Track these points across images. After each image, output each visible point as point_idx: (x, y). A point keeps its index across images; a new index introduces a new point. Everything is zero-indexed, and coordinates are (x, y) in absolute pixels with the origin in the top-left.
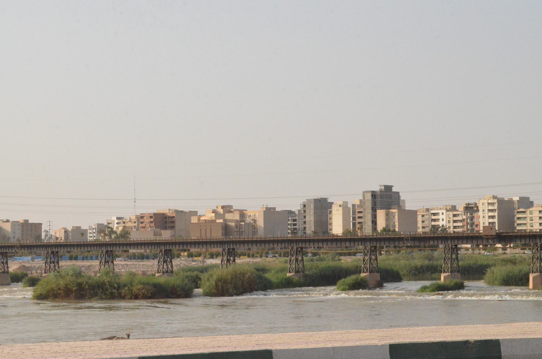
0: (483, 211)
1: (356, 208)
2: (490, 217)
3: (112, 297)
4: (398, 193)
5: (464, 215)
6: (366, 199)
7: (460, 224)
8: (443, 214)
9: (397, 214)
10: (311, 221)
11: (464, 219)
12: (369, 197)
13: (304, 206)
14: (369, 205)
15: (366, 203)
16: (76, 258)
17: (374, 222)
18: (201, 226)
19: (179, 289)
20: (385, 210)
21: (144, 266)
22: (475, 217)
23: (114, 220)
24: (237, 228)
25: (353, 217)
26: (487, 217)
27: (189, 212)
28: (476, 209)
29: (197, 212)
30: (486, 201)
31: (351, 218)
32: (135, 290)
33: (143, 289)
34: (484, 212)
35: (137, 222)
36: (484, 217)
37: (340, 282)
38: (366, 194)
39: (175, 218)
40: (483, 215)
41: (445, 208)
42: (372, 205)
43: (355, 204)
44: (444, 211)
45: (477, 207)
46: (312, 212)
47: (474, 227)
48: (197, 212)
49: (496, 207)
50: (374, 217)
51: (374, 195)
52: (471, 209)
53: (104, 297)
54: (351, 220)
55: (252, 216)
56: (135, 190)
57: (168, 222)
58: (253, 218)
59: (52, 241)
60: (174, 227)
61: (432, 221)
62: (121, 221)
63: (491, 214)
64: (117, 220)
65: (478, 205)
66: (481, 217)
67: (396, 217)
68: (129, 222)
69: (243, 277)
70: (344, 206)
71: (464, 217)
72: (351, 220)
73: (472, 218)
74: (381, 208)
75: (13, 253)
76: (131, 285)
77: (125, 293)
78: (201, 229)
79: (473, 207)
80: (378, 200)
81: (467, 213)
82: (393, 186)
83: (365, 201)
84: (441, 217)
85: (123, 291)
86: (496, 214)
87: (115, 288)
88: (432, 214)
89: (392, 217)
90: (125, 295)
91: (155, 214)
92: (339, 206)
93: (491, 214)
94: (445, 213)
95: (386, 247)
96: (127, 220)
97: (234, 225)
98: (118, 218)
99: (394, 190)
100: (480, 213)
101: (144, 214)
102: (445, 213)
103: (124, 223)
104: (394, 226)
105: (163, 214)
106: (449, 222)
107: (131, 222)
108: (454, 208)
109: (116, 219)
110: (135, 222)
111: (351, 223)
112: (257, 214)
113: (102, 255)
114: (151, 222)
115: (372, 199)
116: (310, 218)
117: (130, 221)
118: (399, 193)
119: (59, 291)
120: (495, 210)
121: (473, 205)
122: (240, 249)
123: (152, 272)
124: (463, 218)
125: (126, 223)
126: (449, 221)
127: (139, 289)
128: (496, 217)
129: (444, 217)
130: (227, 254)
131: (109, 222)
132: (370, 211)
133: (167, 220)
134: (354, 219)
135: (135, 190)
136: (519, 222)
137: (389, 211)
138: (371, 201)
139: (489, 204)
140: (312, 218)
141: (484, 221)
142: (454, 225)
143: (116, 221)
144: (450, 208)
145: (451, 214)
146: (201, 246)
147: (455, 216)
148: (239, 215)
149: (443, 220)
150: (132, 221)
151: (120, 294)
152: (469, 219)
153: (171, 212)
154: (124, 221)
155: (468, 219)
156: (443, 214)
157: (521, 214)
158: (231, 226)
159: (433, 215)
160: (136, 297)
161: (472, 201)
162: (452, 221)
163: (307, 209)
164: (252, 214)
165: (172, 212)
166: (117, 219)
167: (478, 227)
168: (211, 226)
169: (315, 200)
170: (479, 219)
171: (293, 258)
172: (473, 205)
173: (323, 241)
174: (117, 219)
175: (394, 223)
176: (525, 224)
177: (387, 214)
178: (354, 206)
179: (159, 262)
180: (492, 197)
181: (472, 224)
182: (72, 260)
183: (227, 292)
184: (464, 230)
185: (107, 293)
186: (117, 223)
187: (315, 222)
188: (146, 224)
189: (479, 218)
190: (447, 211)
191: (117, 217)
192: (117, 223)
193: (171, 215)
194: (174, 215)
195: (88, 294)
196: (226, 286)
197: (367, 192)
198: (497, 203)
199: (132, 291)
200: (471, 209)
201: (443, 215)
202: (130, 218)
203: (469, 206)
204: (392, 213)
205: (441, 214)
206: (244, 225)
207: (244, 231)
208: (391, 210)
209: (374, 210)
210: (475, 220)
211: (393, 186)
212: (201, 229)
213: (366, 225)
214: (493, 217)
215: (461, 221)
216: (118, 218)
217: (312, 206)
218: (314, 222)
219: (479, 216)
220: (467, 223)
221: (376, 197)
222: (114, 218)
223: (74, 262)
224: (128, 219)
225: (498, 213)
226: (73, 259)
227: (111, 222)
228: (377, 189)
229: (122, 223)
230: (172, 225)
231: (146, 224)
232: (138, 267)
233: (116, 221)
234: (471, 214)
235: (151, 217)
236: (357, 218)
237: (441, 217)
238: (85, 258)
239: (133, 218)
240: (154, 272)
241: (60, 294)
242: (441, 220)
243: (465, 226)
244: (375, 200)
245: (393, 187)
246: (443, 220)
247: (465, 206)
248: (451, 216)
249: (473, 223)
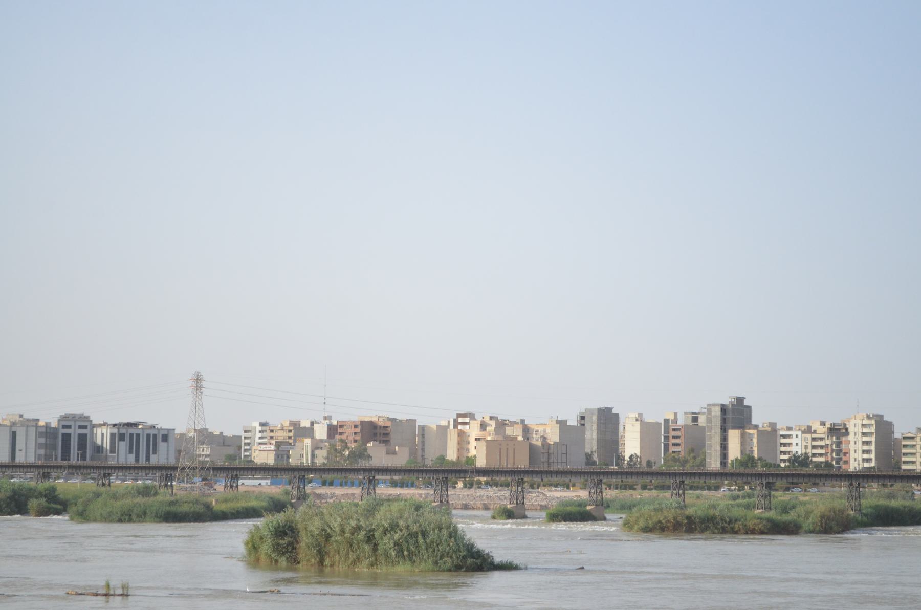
0: (855, 434)
1: (670, 424)
2: (864, 443)
3: (724, 531)
5: (828, 439)
6: (713, 414)
7: (823, 451)
8: (797, 436)
9: (756, 436)
10: (592, 439)
11: (828, 444)
12: (717, 411)
13: (583, 418)
14: (717, 422)
15: (713, 420)
16: (331, 484)
17: (724, 447)
18: (500, 445)
19: (792, 525)
20: (740, 431)
21: (469, 496)
22: (843, 443)
23: (256, 427)
24: (544, 449)
25: (664, 436)
26: (860, 444)
27: (407, 420)
28: (844, 431)
29: (416, 420)
30: (859, 422)
31: (663, 437)
32: (750, 524)
33: (761, 523)
34: (856, 437)
35: (293, 431)
36: (855, 443)
38: (713, 408)
39: (389, 429)
40: (855, 440)
41: (798, 429)
42: (721, 423)
43: (669, 419)
44: (799, 433)
45: (847, 429)
46: (595, 426)
47: (842, 455)
48: (416, 420)
49: (873, 430)
51: (724, 409)
52: (838, 431)
53: (716, 531)
54: (663, 441)
55: (540, 431)
56: (325, 386)
57: (378, 435)
58: (542, 435)
59: (523, 467)
60: (389, 441)
61: (781, 446)
62: (264, 428)
63: (866, 439)
64: (260, 427)
65: (847, 426)
66: (852, 443)
67: (755, 440)
68: (280, 431)
69: (843, 514)
70: (639, 418)
71: (828, 442)
72: (661, 440)
73: (839, 444)
74: (734, 428)
76: (746, 520)
77: (739, 527)
78: (500, 449)
79: (840, 429)
80: (729, 416)
81: (832, 436)
82: (745, 398)
83: (711, 418)
84: (793, 441)
85: (736, 526)
86: (873, 439)
87: (726, 522)
88: (781, 435)
89: (749, 440)
90: (740, 530)
91: (362, 423)
92: (635, 420)
93: (866, 439)
94: (800, 436)
95: (805, 483)
96: (277, 427)
97: (540, 445)
98: (262, 425)
99: (746, 403)
100: (851, 437)
101: (345, 422)
102: (800, 436)
103: (272, 431)
104: (752, 452)
106: (806, 447)
107: (283, 431)
109: (258, 424)
110: (290, 431)
111: (662, 445)
112: (548, 430)
113: (39, 477)
114: (355, 433)
115: (721, 414)
116: (591, 436)
117: (282, 429)
118: (751, 408)
119: (669, 524)
120: (870, 434)
121: (841, 426)
122: (779, 483)
123: (496, 505)
124: (827, 443)
125: (276, 432)
126: (805, 446)
127: (755, 524)
128: (874, 444)
129: (799, 441)
130: (764, 488)
131: (247, 430)
133: (378, 431)
134: (666, 438)
135: (325, 386)
136: (904, 451)
137: (744, 431)
138: (720, 418)
139: (863, 425)
140: (595, 436)
141: (856, 448)
142: (813, 452)
143: (259, 428)
144: (804, 429)
145: (809, 436)
146: (664, 477)
147: (814, 439)
148: (522, 429)
149: (797, 444)
150: (285, 428)
151: (732, 528)
152: (834, 445)
153: (381, 419)
154: (271, 429)
155: (832, 444)
156: (797, 436)
157: (908, 440)
158: (536, 445)
159: (783, 438)
160: (753, 532)
161: (838, 421)
162: (810, 447)
163: (586, 422)
164: (540, 429)
165: (384, 420)
167: (847, 455)
168: (507, 445)
169: (598, 409)
170: (850, 445)
171: (514, 489)
172: (841, 426)
173: (890, 477)
175: (751, 448)
176: (914, 454)
177: (743, 436)
178: (666, 421)
179: (363, 489)
180: (865, 416)
181: (838, 452)
182: (325, 485)
183: (831, 528)
184: (827, 459)
185: (719, 527)
186: (260, 432)
187: (599, 441)
188: (347, 437)
189: (849, 443)
190: (804, 432)
191: (260, 423)
192: (260, 432)
194: (388, 424)
195: (698, 529)
196: (401, 530)
197: (714, 405)
198: (874, 426)
199: (746, 525)
200: (838, 431)
201: (797, 439)
202: (282, 424)
203: (836, 427)
204: (749, 434)
205: (794, 436)
206: (554, 444)
207: (553, 453)
208: (747, 431)
209: (724, 430)
210: (843, 446)
211: (745, 398)
212: (500, 449)
213: (712, 449)
214: (868, 443)
215: (822, 447)
216: (262, 425)
217: (595, 418)
218: (598, 441)
219: (849, 441)
220: (832, 451)
221: (727, 413)
222: (256, 424)
223: (628, 493)
224: (279, 426)
225: (876, 438)
226: (327, 484)
227: (250, 430)
228: (726, 401)
229: (269, 431)
230: (385, 439)
231: (347, 437)
232: (462, 499)
233: (259, 428)
234: (838, 438)
235: (356, 426)
236: (671, 438)
237: (793, 441)
238: (344, 484)
239: (287, 424)
240: (498, 506)
241: (668, 528)
242: (794, 444)
243: (829, 454)
244: (725, 416)
245: (745, 400)
246: (797, 444)
247: (829, 426)
248: (810, 440)
249: (841, 451)
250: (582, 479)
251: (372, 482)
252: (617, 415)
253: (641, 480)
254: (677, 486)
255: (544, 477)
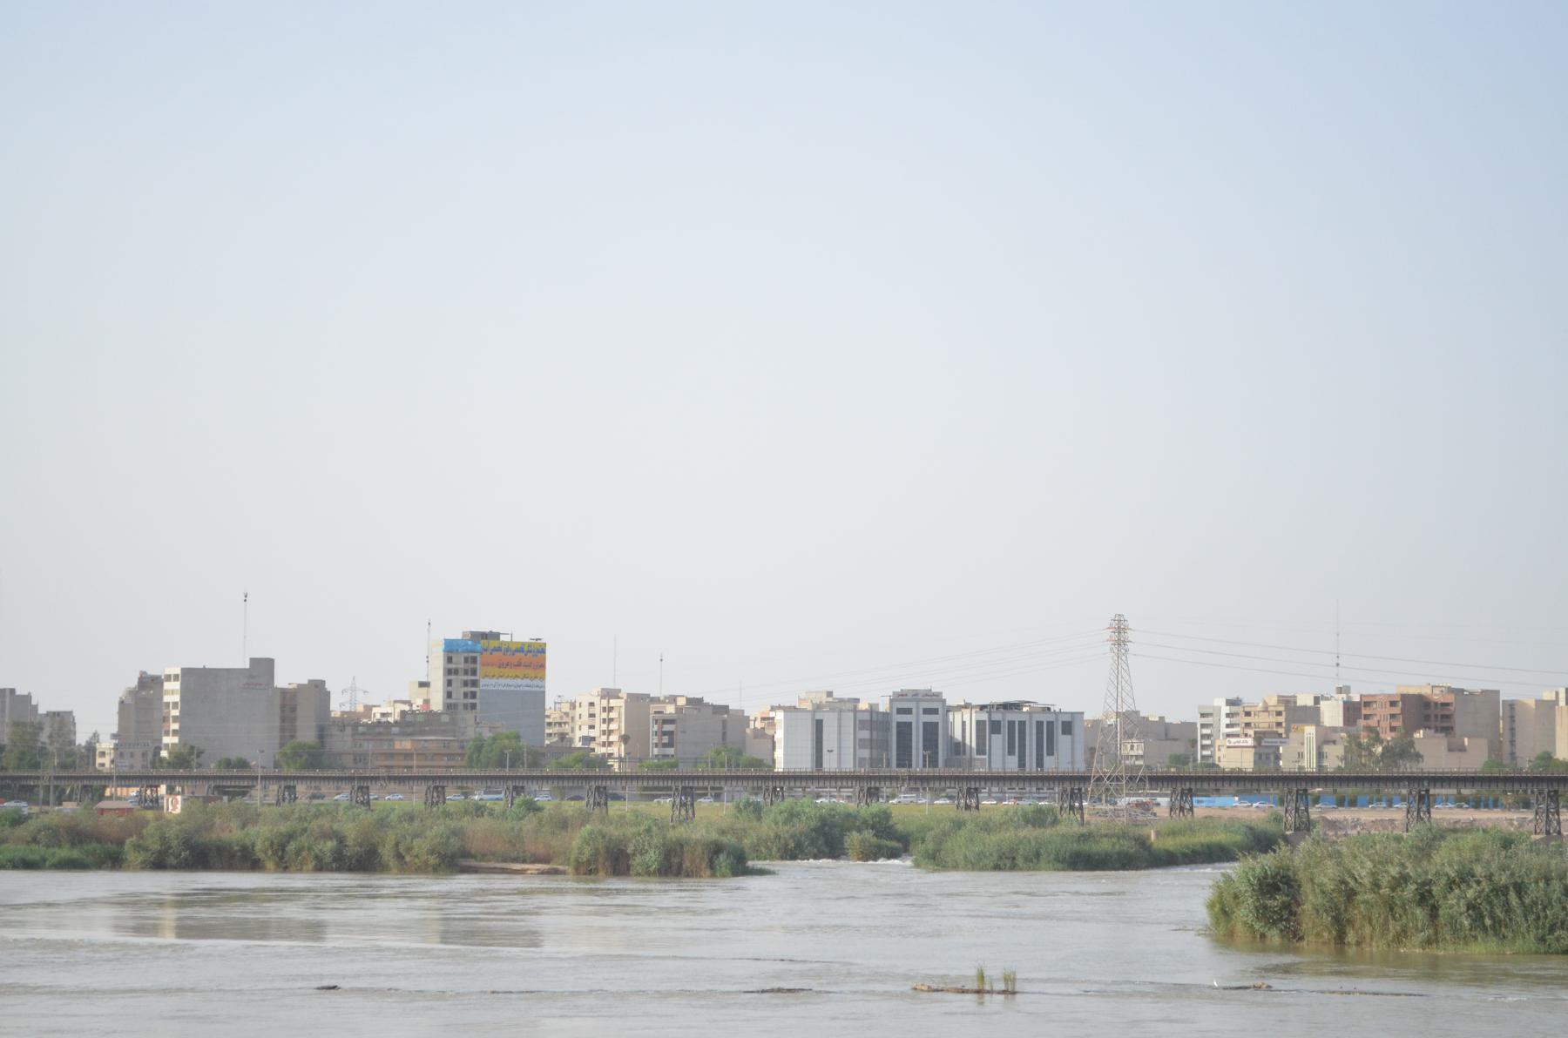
16: (1353, 803)
23: (1220, 707)
27: (1483, 692)
35: (1284, 713)
39: (1452, 708)
57: (1433, 718)
60: (1452, 728)
62: (1234, 709)
68: (1261, 714)
75: (1205, 790)
91: (1404, 697)
98: (1230, 703)
103: (1248, 714)
105: (1420, 697)
110: (1279, 713)
114: (1393, 716)
143: (1226, 709)
150: (1270, 709)
153: (1436, 691)
165: (1442, 691)
166: (1227, 705)
174: (1227, 705)
179: (1408, 812)
186: (1228, 715)
188: (1379, 722)
192: (1228, 715)
193: (1442, 701)
194: (1450, 698)
196: (1478, 883)
202: (1265, 702)
216: (1230, 703)
222: (1220, 702)
224: (1261, 705)
226: (1346, 803)
229: (1243, 714)
230: (1445, 725)
231: (1379, 722)
233: (1226, 709)
235: (1393, 704)
239: (1273, 701)
252: (310, 681)
254: (864, 795)
255: (1382, 786)
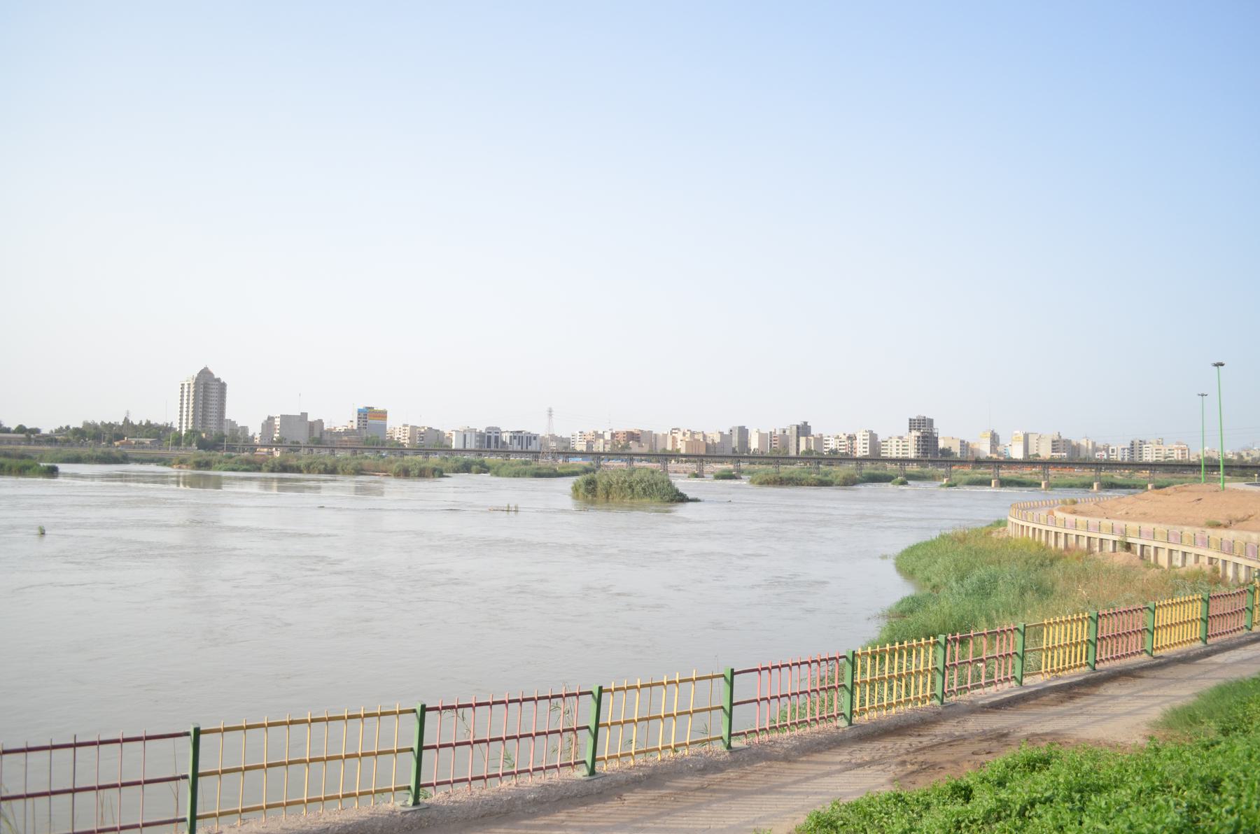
3: (797, 484)
4: (810, 426)
7: (844, 447)
13: (731, 431)
17: (798, 445)
30: (862, 434)
32: (810, 482)
37: (893, 481)
44: (833, 439)
46: (737, 435)
49: (868, 437)
50: (798, 441)
51: (798, 427)
52: (852, 438)
67: (812, 442)
70: (758, 431)
73: (852, 444)
80: (801, 430)
84: (830, 442)
86: (868, 442)
98: (580, 432)
99: (808, 424)
100: (858, 441)
104: (811, 447)
108: (838, 437)
116: (735, 439)
132: (795, 437)
134: (771, 441)
136: (883, 447)
140: (737, 440)
143: (579, 434)
145: (838, 440)
147: (840, 442)
160: (811, 485)
161: (852, 433)
164: (711, 435)
169: (739, 427)
176: (887, 449)
178: (771, 433)
181: (852, 448)
187: (739, 442)
194: (640, 433)
200: (852, 438)
209: (798, 437)
214: (866, 444)
216: (580, 432)
217: (737, 431)
222: (577, 432)
223: (753, 466)
234: (852, 441)
235: (624, 434)
237: (830, 442)
239: (592, 432)
250: (730, 460)
251: (632, 460)
253: (758, 460)
